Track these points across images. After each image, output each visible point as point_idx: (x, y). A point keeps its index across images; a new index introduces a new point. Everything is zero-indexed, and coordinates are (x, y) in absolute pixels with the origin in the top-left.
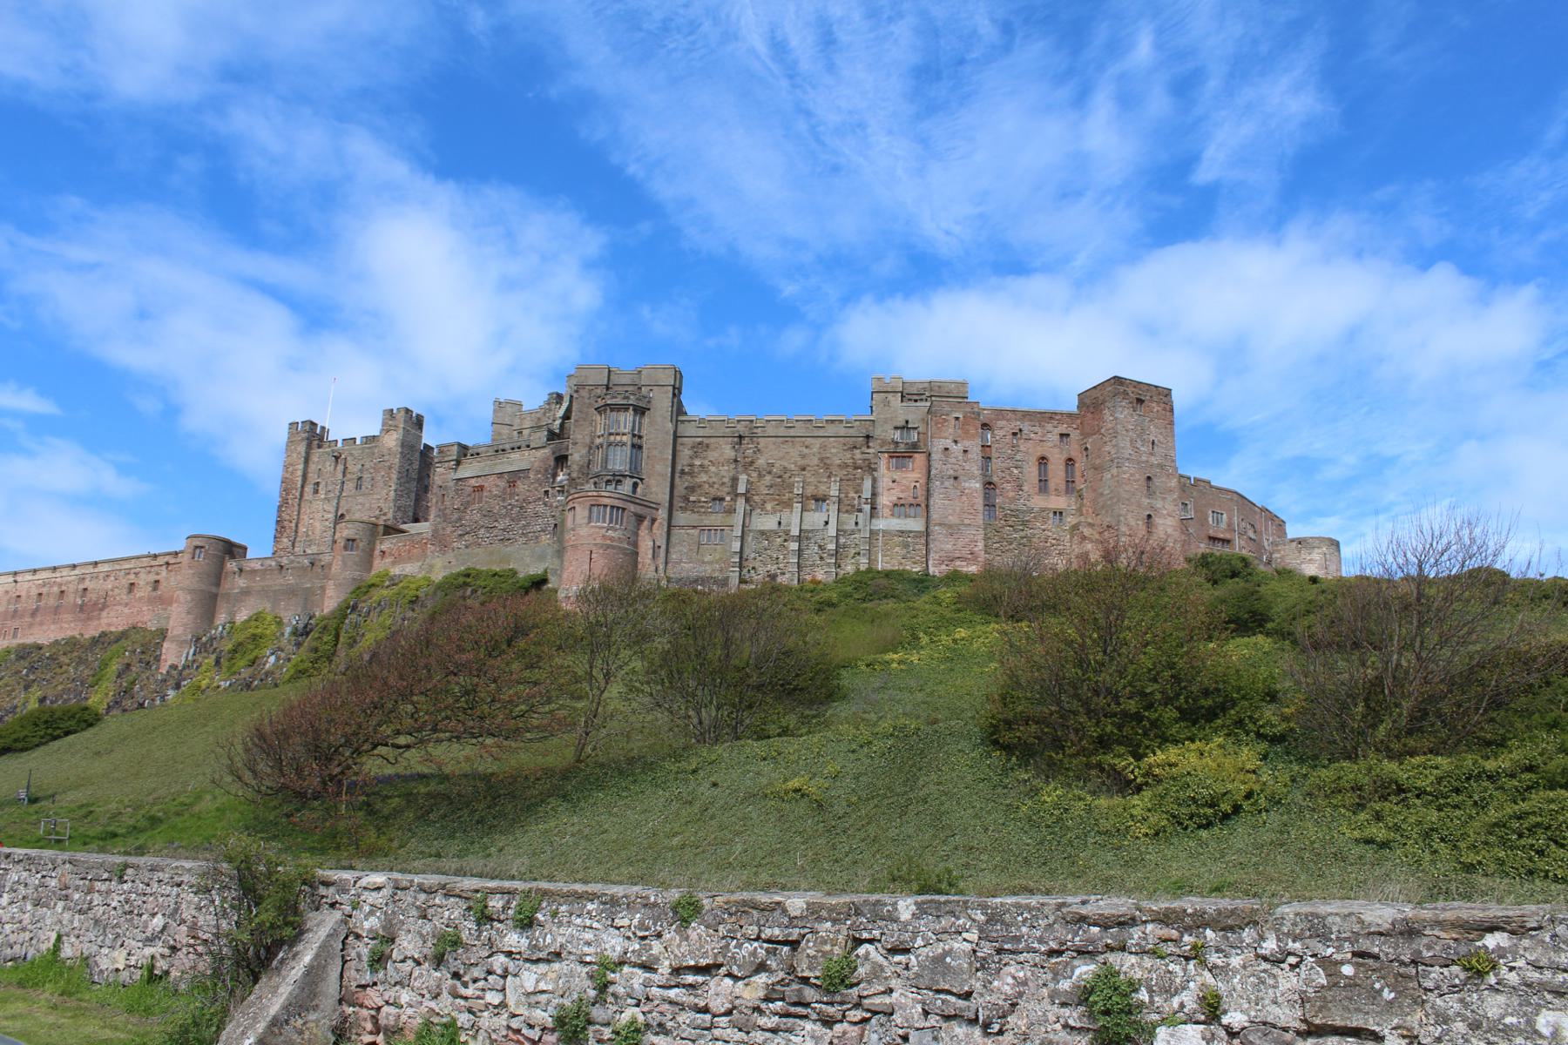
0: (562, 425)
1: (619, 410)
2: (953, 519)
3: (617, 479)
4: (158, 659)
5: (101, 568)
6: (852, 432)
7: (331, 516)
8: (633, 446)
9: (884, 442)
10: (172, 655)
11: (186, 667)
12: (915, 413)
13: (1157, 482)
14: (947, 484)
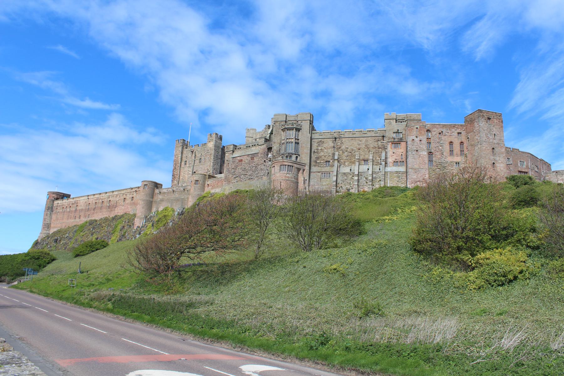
0: (270, 137)
1: (290, 130)
2: (416, 167)
3: (290, 156)
4: (133, 224)
5: (116, 193)
6: (377, 135)
7: (191, 173)
8: (296, 143)
9: (389, 138)
10: (138, 223)
11: (142, 227)
12: (401, 127)
13: (496, 150)
14: (414, 153)
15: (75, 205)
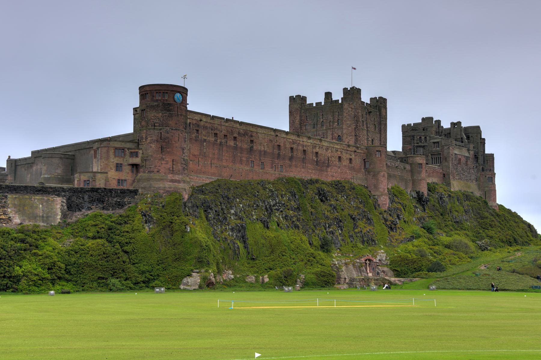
15: (247, 139)
